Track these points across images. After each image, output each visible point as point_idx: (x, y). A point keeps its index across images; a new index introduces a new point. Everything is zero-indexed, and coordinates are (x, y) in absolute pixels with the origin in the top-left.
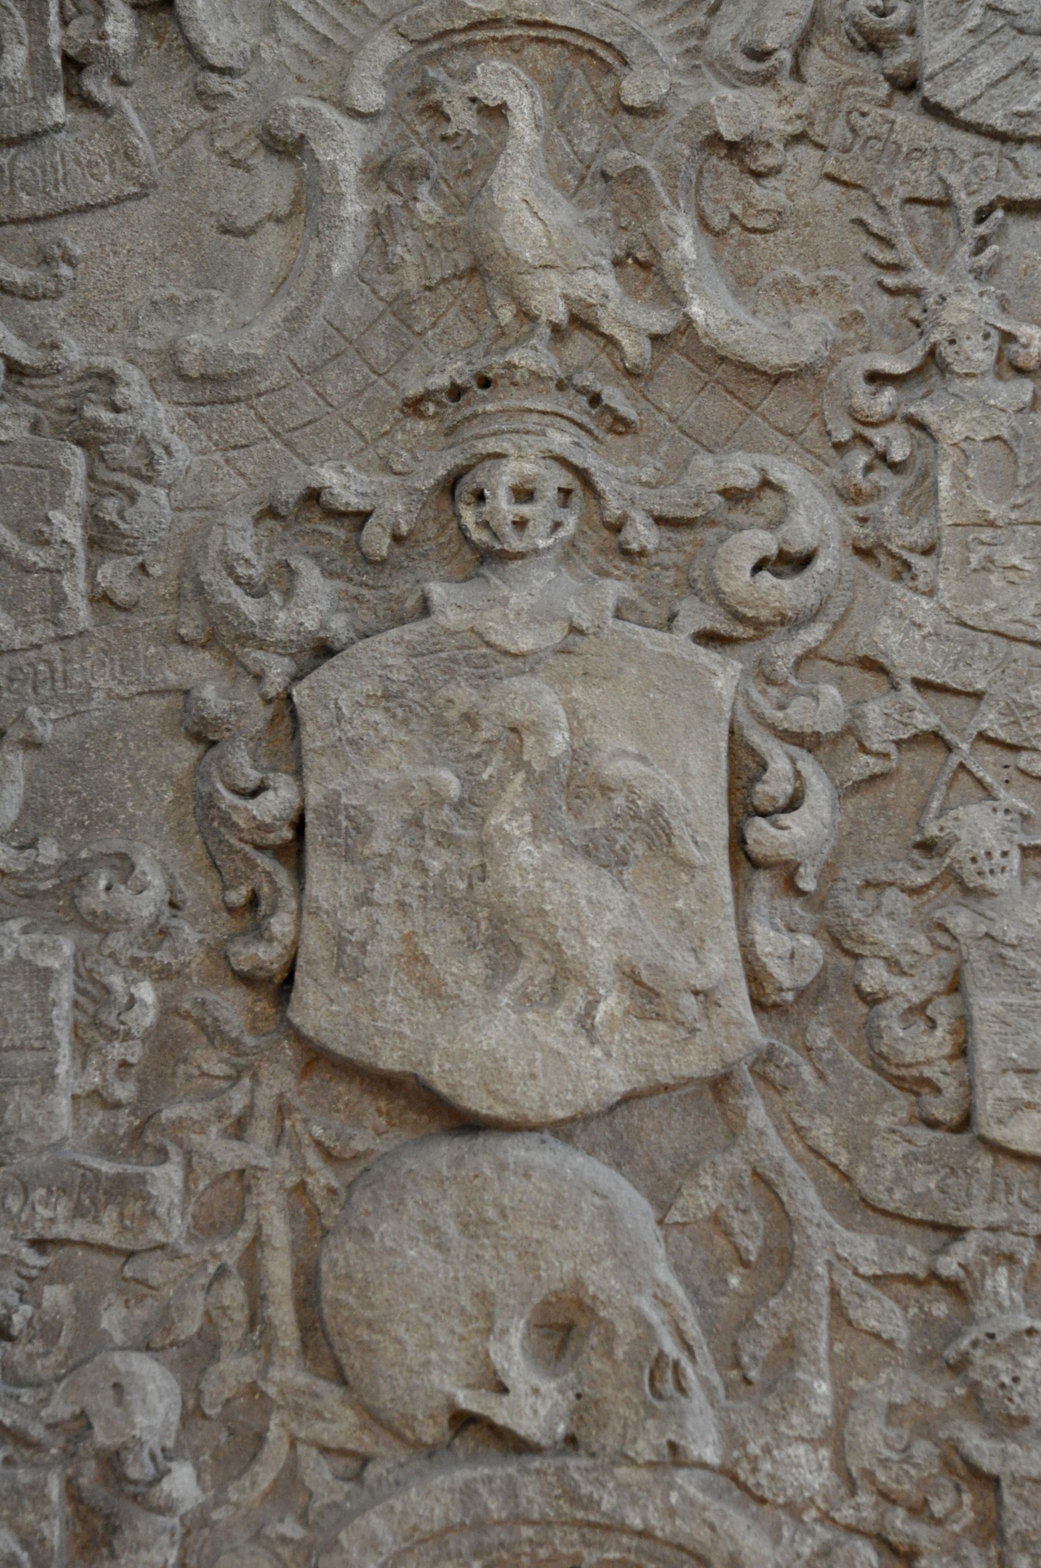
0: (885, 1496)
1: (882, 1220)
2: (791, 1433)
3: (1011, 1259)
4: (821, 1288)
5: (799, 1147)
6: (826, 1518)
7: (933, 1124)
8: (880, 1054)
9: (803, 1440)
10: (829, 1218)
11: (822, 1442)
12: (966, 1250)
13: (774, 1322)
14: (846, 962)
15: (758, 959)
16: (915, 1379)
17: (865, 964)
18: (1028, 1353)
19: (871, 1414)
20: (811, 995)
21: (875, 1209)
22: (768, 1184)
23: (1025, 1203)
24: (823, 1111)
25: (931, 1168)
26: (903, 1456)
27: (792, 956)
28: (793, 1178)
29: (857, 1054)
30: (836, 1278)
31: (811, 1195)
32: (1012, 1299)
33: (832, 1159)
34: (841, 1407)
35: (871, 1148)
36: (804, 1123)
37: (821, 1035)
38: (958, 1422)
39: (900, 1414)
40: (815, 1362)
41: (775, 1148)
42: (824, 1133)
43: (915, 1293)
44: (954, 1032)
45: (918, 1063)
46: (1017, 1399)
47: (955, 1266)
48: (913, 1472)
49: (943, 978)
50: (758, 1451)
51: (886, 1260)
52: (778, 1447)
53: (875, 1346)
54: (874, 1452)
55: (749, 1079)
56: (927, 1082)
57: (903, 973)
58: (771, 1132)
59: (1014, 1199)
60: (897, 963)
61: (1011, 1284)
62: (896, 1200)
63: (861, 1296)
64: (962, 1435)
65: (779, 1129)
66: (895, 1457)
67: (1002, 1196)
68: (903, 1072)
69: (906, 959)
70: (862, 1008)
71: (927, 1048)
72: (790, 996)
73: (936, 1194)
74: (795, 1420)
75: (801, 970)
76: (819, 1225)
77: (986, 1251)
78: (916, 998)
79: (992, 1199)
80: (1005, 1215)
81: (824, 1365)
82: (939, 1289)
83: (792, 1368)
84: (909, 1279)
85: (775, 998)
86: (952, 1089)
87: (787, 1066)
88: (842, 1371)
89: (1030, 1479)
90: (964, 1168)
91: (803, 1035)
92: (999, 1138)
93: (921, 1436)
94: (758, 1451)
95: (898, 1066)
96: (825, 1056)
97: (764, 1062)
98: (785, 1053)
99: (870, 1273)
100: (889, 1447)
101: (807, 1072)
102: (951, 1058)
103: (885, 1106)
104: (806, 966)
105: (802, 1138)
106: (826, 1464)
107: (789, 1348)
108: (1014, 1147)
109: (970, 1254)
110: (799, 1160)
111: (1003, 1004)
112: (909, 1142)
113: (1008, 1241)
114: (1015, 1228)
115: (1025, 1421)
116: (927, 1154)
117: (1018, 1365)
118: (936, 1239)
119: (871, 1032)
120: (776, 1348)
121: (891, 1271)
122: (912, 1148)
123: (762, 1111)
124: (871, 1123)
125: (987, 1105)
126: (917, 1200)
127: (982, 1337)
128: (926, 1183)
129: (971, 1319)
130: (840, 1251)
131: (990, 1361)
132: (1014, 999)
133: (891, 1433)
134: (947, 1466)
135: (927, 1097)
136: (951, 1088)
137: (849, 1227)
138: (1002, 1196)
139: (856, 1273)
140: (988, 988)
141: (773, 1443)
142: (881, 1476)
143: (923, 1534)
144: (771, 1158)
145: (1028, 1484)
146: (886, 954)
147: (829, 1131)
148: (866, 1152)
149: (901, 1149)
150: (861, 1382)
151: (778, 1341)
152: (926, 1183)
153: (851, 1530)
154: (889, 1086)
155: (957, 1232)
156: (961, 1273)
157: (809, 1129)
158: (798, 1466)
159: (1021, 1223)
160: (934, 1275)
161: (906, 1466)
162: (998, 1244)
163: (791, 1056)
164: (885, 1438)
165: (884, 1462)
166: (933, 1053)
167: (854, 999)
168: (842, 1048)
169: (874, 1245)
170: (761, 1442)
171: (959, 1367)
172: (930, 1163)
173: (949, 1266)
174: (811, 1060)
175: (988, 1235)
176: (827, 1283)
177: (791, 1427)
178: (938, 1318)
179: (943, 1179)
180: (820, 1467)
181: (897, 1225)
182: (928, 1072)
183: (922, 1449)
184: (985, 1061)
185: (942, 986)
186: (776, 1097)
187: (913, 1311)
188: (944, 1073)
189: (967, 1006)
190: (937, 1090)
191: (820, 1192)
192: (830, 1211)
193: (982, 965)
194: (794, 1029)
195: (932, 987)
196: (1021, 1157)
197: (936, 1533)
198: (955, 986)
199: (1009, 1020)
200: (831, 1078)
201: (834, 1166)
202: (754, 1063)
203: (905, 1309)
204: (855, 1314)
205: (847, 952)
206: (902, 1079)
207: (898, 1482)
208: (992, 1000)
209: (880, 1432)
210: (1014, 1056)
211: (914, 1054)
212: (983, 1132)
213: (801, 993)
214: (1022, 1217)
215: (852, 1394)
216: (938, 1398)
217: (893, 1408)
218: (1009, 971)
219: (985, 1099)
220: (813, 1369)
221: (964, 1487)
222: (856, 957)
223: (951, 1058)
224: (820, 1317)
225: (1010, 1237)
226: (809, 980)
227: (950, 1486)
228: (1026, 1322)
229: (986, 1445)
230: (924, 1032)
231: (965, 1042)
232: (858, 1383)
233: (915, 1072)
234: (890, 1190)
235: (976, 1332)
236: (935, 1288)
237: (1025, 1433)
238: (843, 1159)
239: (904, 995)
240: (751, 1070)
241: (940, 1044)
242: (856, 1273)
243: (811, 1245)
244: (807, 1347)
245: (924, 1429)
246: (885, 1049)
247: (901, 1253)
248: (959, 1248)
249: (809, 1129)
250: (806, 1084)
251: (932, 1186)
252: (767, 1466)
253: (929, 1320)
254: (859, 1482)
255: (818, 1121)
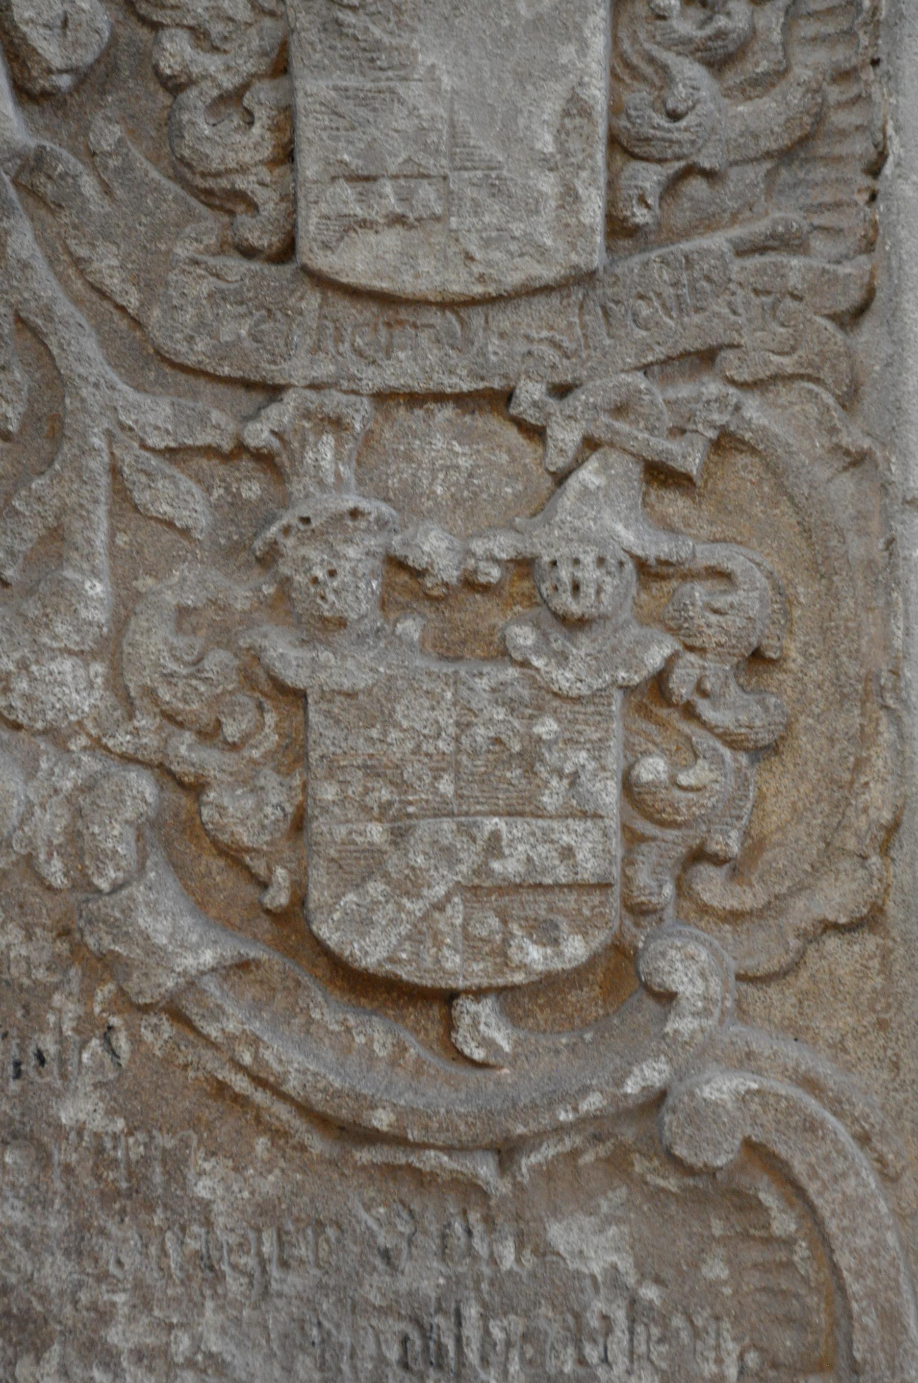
0: (170, 717)
1: (182, 377)
2: (55, 645)
3: (337, 424)
4: (97, 465)
5: (78, 285)
6: (97, 746)
7: (249, 253)
8: (182, 160)
9: (70, 653)
10: (113, 376)
11: (95, 655)
12: (281, 414)
13: (38, 507)
14: (144, 33)
15: (16, 28)
16: (215, 576)
17: (165, 36)
18: (349, 541)
19: (156, 620)
20: (97, 78)
21: (173, 365)
22: (35, 332)
23: (359, 353)
24: (107, 237)
25: (242, 309)
26: (192, 669)
27: (65, 24)
28: (67, 325)
29: (155, 161)
30: (117, 452)
31: (90, 346)
32: (337, 475)
33: (119, 300)
34: (123, 612)
35: (167, 284)
36: (83, 252)
37: (107, 134)
38: (264, 629)
39: (194, 619)
40: (88, 557)
41: (45, 285)
42: (107, 264)
43: (221, 470)
44: (275, 128)
45: (228, 171)
46: (331, 597)
47: (266, 435)
48: (202, 689)
49: (265, 54)
50: (12, 667)
51: (183, 429)
52: (37, 662)
53: (168, 537)
54: (157, 665)
55: (12, 193)
56: (241, 196)
57: (215, 49)
58: (40, 265)
59: (345, 347)
60: (206, 35)
61: (338, 457)
62: (199, 351)
63: (148, 474)
64: (266, 643)
65: (52, 262)
66: (184, 671)
67: (329, 344)
68: (210, 183)
69: (217, 29)
70: (164, 99)
71: (238, 150)
72: (65, 81)
73: (248, 344)
74: (60, 629)
75: (76, 43)
76: (96, 385)
77: (307, 415)
78: (228, 82)
79: (317, 348)
80: (332, 368)
81: (102, 561)
82: (251, 465)
83: (60, 566)
84: (210, 451)
85: (43, 83)
86: (272, 205)
87: (62, 176)
88: (126, 569)
89: (340, 693)
90: (283, 310)
91: (86, 136)
92: (325, 269)
93: (218, 644)
94: (12, 667)
95: (203, 175)
96: (112, 163)
97: (32, 171)
98: (58, 159)
99: (162, 445)
100: (177, 659)
101: (89, 185)
102: (273, 163)
103: (188, 230)
104: (83, 38)
105: (82, 273)
106: (99, 680)
107: (56, 539)
108: (344, 280)
109: (286, 419)
110: (77, 301)
111: (336, 88)
112: (218, 276)
113: (334, 401)
114: (345, 384)
115: (342, 623)
116: (237, 292)
117: (336, 555)
118: (247, 401)
119: (171, 128)
120: (42, 540)
121: (189, 442)
122: (222, 285)
123: (30, 236)
124: (169, 251)
125: (310, 225)
126: (224, 352)
127: (295, 522)
128: (236, 329)
129: (286, 502)
130: (123, 418)
131: (303, 551)
132: (352, 81)
133: (180, 642)
134: (248, 680)
135: (243, 218)
136: (269, 203)
137: (137, 388)
138: (329, 344)
139: (144, 446)
140: (319, 68)
141: (32, 657)
142: (165, 694)
143: (211, 761)
144: (37, 298)
145: (338, 698)
146: (192, 22)
147: (115, 262)
148: (161, 290)
149: (206, 286)
150: (150, 581)
151: (43, 532)
152: (236, 329)
153: (128, 759)
154: (194, 202)
155: (274, 391)
156: (276, 443)
157: (89, 261)
158: (62, 684)
159: (352, 378)
160: (241, 448)
161: (194, 682)
162: (322, 405)
163: (68, 162)
164: (172, 649)
165: (169, 678)
166: (247, 157)
167: (153, 86)
168: (135, 152)
169: (169, 411)
170: (17, 656)
171: (269, 559)
172: (242, 303)
173: (259, 434)
174: (95, 168)
175: (310, 394)
176: (106, 459)
177: (55, 637)
178: (248, 501)
179: (257, 325)
180: (91, 685)
181: (201, 384)
182: (241, 183)
183: (218, 660)
184: (310, 166)
185: (263, 65)
186: (50, 219)
187: (218, 492)
188: (262, 184)
189: (292, 91)
190: (253, 207)
191: (103, 343)
192: (115, 367)
193: (312, 35)
194: (74, 127)
195: (249, 67)
196: (355, 293)
197: (229, 759)
198: (280, 67)
199: (341, 110)
200: (119, 193)
201: (122, 309)
202: (18, 173)
203: (209, 490)
204: (141, 497)
205: (144, 21)
206: (209, 192)
207: (186, 702)
208: (322, 83)
209: (166, 641)
210: (346, 158)
211: (223, 159)
212: (305, 260)
213: (82, 76)
214: (353, 370)
215: (139, 595)
216: (241, 597)
217: (183, 611)
218: (349, 43)
219: (308, 217)
220: (85, 566)
221: (268, 705)
222: (156, 27)
223: (273, 163)
224: (96, 501)
225: (337, 396)
226: (89, 58)
227: (252, 705)
228: (351, 501)
229: (293, 654)
230: (237, 129)
231: (291, 141)
232: (146, 583)
233: (224, 183)
234: (190, 339)
235: (289, 518)
236: (246, 463)
237: (340, 638)
238: (133, 300)
239: (214, 79)
240: (15, 182)
241: (256, 146)
242: (144, 446)
243: (85, 411)
244: (79, 538)
245: (223, 636)
246: (187, 153)
247: (203, 419)
248: (273, 411)
249: (89, 261)
250: (85, 201)
251: (243, 332)
252: (23, 685)
253: (236, 503)
254: (137, 702)
255: (100, 250)
